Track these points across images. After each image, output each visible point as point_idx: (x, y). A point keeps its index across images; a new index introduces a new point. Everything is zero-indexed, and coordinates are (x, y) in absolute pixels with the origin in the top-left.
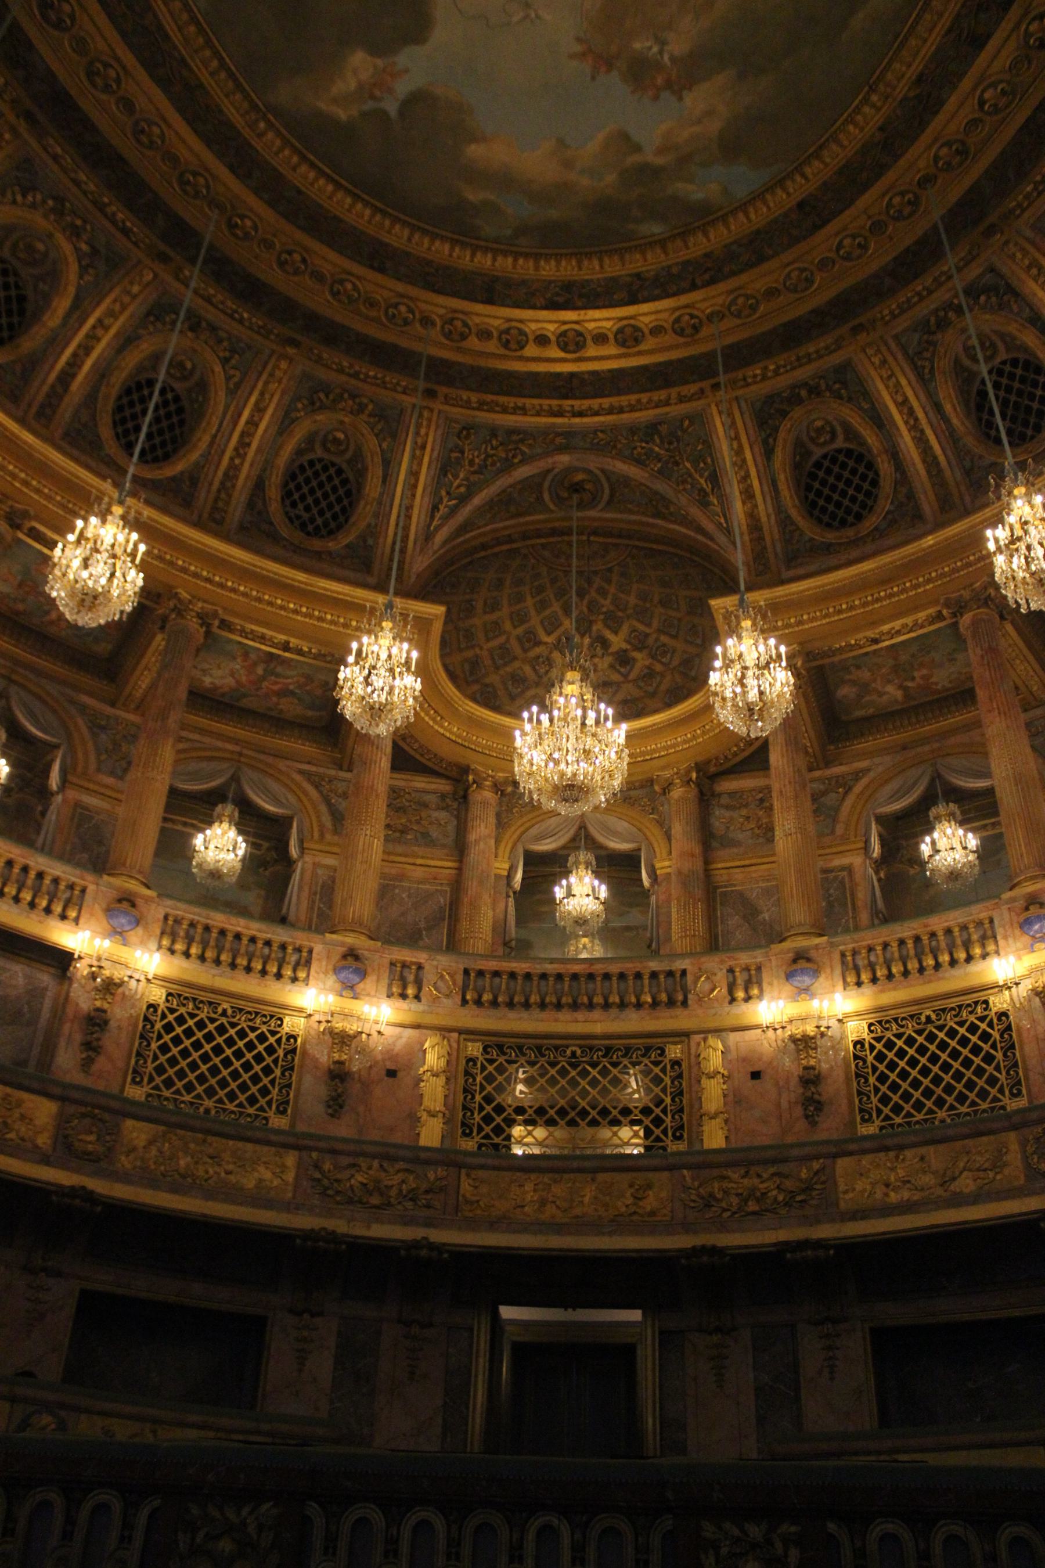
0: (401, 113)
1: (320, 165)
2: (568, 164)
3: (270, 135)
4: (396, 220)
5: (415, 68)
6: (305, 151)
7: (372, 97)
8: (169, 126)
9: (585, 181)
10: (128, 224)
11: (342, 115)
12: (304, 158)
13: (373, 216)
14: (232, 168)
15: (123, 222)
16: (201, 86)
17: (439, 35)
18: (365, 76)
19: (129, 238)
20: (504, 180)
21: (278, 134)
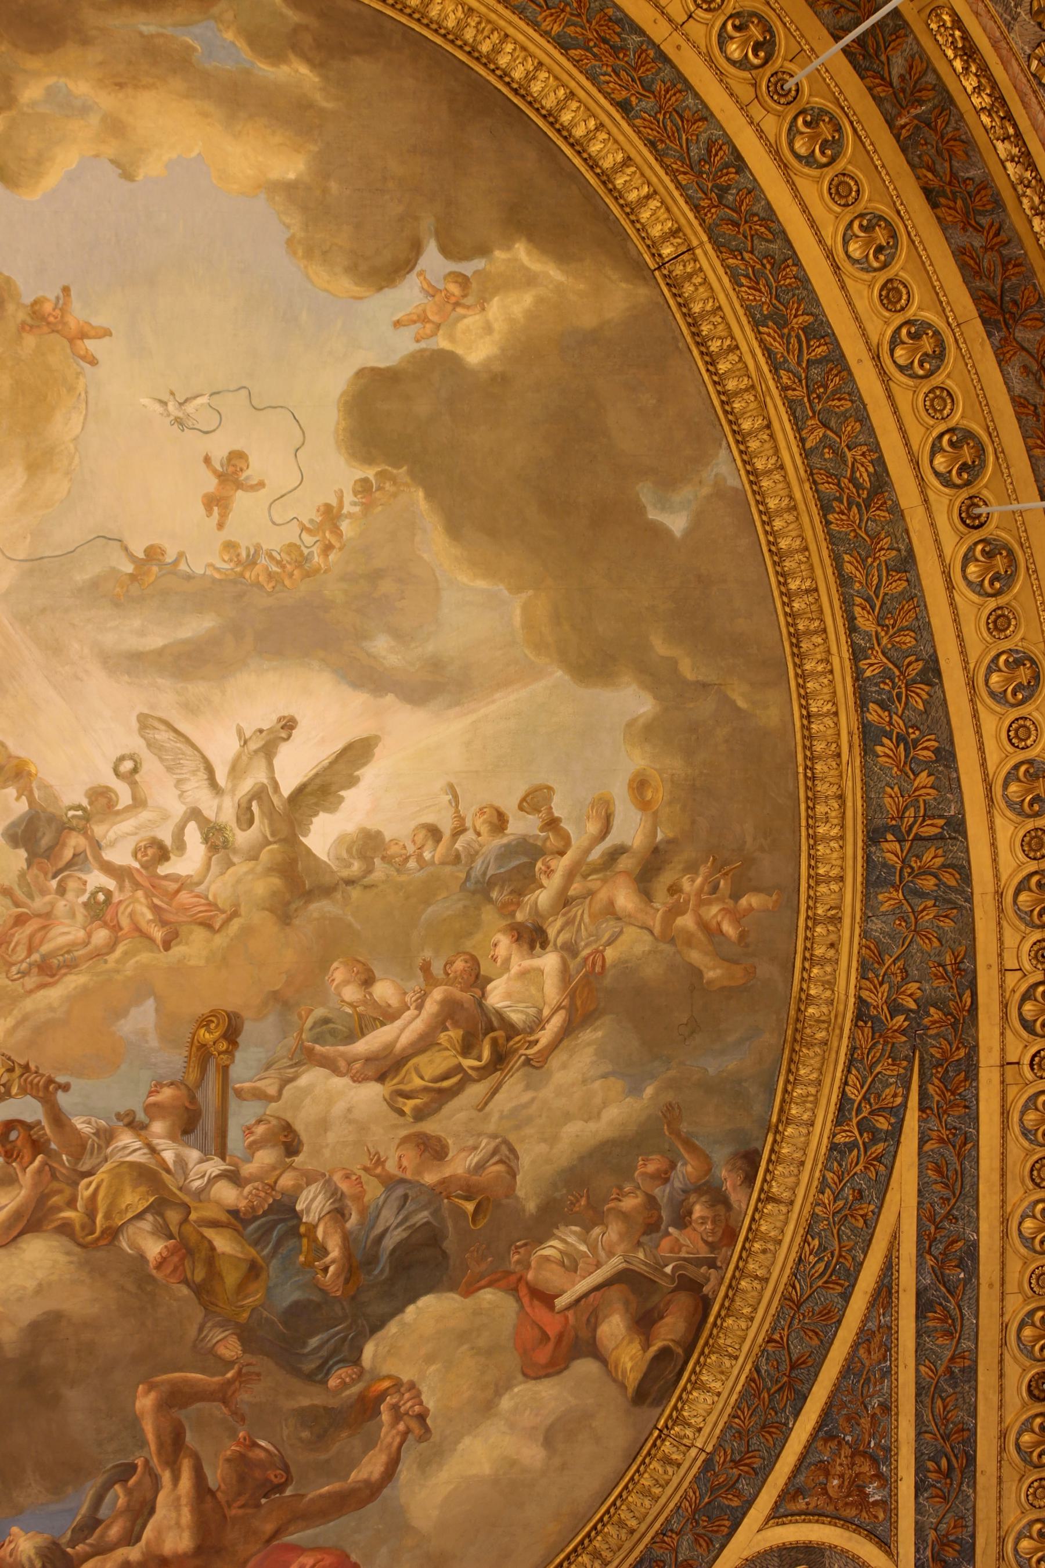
0: (417, 248)
1: (577, 161)
2: (115, 127)
3: (656, 231)
4: (453, 37)
5: (383, 328)
6: (601, 190)
7: (464, 281)
8: (830, 255)
9: (82, 88)
10: (958, 64)
11: (522, 252)
12: (606, 179)
13: (496, 50)
14: (739, 163)
15: (966, 69)
16: (756, 324)
17: (335, 382)
18: (472, 321)
19: (966, 37)
20: (236, 100)
21: (642, 230)
